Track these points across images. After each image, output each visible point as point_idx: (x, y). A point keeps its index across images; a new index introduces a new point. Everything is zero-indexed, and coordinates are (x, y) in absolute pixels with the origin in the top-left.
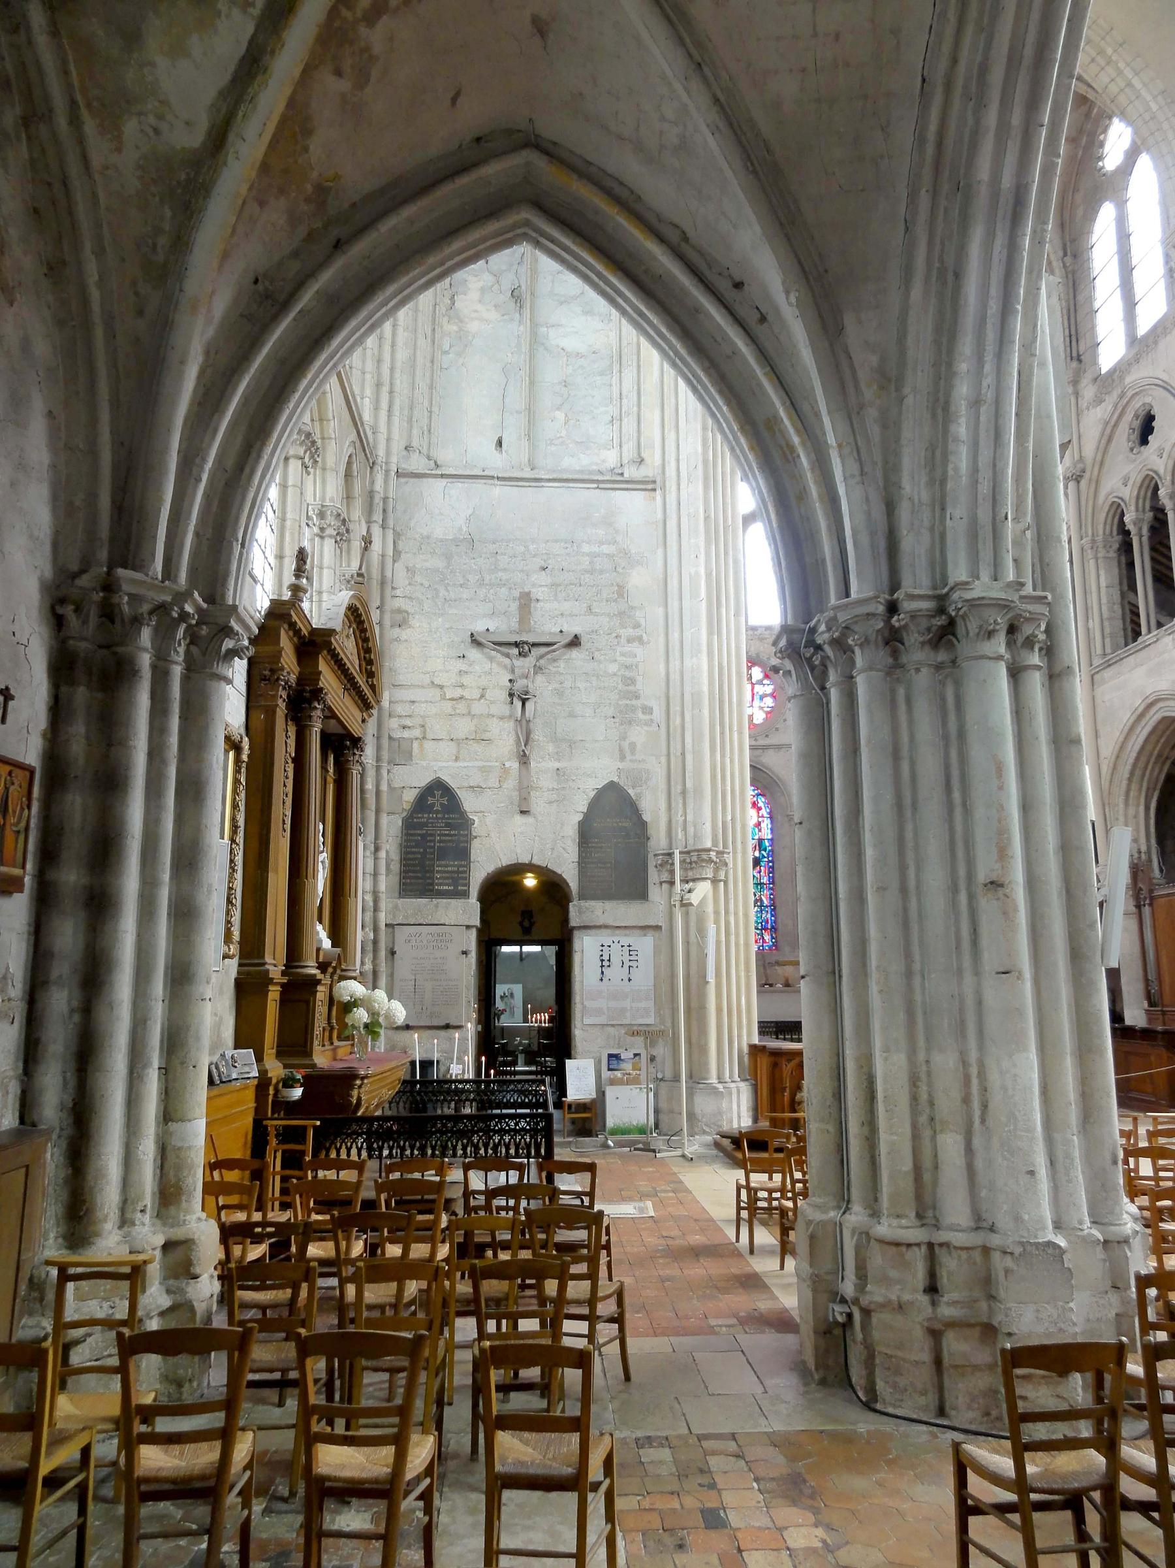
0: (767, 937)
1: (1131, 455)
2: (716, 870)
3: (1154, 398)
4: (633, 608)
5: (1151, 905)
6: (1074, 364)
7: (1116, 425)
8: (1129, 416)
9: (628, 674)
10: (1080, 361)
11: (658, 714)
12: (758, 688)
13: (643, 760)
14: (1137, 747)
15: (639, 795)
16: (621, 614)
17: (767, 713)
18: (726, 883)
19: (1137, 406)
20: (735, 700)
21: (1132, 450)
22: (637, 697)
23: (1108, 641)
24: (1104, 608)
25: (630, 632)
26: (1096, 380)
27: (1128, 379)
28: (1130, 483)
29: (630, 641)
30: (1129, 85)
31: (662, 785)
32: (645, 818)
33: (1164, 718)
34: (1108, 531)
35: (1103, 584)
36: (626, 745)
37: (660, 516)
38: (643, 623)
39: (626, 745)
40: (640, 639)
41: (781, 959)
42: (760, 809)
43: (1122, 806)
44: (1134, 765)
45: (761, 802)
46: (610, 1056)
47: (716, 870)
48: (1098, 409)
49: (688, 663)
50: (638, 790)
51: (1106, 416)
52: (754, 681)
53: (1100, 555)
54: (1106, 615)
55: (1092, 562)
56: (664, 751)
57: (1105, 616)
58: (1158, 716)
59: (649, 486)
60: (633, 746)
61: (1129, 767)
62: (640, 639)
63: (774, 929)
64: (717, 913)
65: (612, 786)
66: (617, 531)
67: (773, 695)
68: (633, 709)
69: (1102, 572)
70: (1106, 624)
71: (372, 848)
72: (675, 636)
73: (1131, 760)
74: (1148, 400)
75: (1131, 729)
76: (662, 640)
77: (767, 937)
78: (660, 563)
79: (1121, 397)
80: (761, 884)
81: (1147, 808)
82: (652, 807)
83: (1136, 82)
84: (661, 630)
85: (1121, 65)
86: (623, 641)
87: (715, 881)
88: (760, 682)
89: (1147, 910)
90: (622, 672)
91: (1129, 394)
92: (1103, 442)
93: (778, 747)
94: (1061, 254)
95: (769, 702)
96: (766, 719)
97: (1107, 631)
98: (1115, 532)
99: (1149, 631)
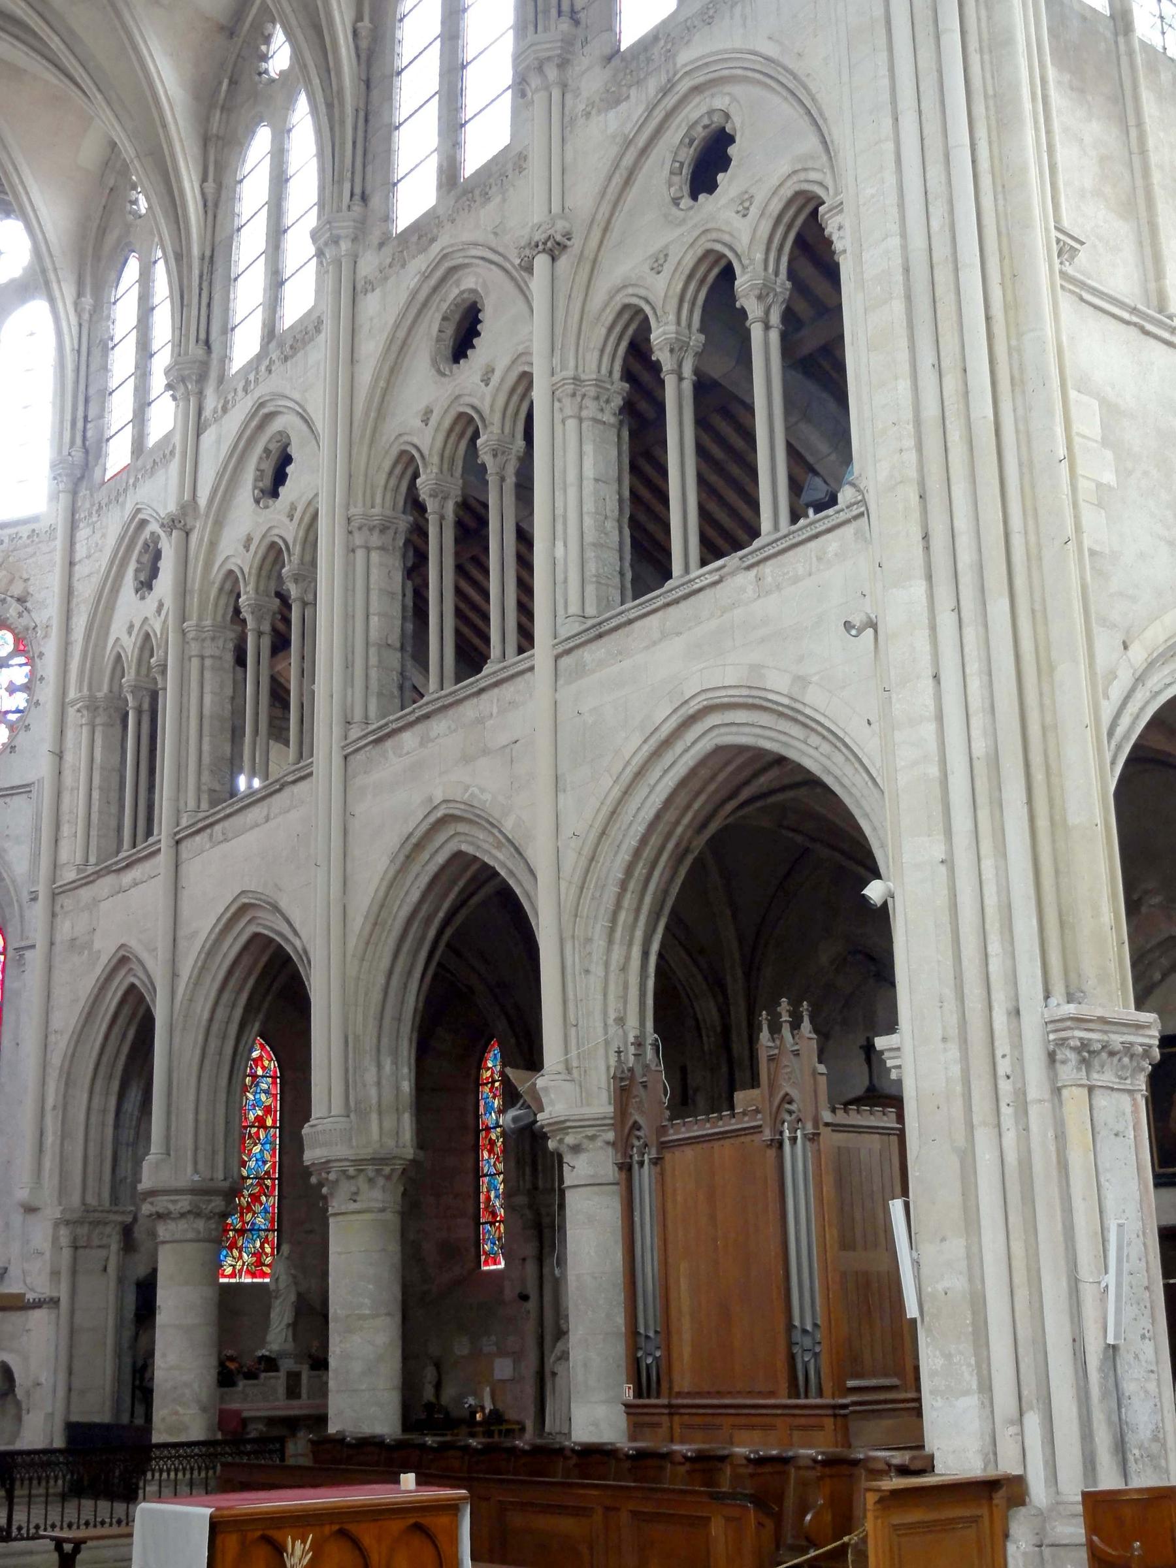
1: (674, 210)
3: (734, 99)
5: (656, 1162)
7: (644, 151)
8: (674, 135)
14: (648, 813)
19: (695, 116)
21: (676, 202)
23: (590, 589)
24: (588, 521)
26: (609, 59)
27: (685, 56)
28: (668, 268)
33: (719, 750)
34: (604, 370)
35: (589, 472)
43: (600, 943)
44: (637, 853)
48: (612, 114)
51: (629, 128)
53: (584, 413)
54: (589, 538)
55: (572, 424)
57: (589, 538)
58: (706, 745)
61: (624, 856)
69: (588, 448)
70: (590, 554)
73: (632, 841)
74: (720, 103)
75: (639, 774)
79: (666, 91)
81: (645, 954)
89: (645, 1176)
91: (684, 86)
92: (618, 180)
97: (591, 568)
98: (617, 374)
99: (687, 570)
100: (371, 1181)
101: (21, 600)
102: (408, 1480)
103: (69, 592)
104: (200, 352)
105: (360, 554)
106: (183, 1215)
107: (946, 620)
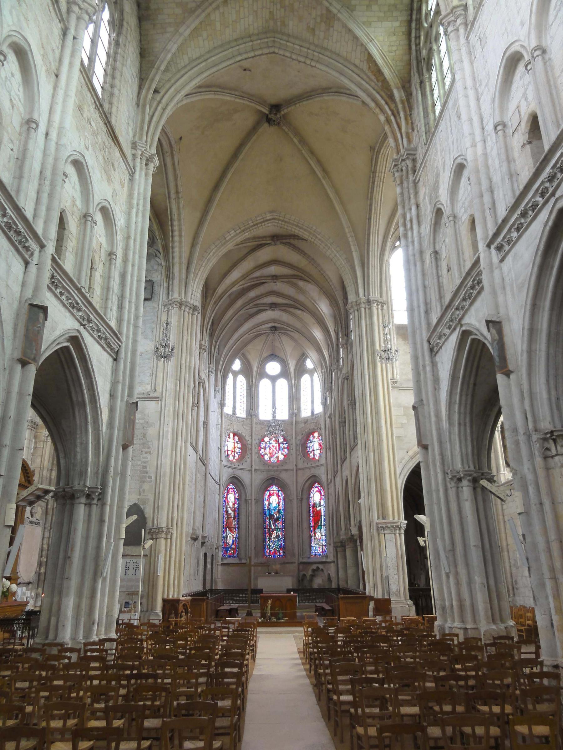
0: (281, 552)
2: (167, 534)
4: (148, 441)
6: (346, 338)
9: (145, 465)
10: (347, 336)
11: (153, 479)
12: (281, 445)
13: (147, 495)
15: (145, 508)
16: (144, 444)
17: (285, 456)
18: (171, 539)
20: (182, 473)
22: (147, 473)
25: (147, 450)
29: (146, 453)
30: (336, 256)
31: (152, 504)
32: (146, 515)
36: (141, 490)
37: (159, 410)
38: (151, 446)
39: (141, 490)
40: (150, 453)
41: (287, 561)
42: (279, 496)
45: (280, 493)
46: (126, 602)
47: (167, 534)
49: (163, 461)
50: (145, 506)
52: (280, 442)
56: (154, 492)
59: (157, 399)
60: (144, 490)
62: (150, 453)
63: (284, 549)
64: (166, 550)
65: (135, 504)
66: (145, 415)
67: (287, 448)
68: (145, 477)
71: (49, 528)
72: (160, 451)
76: (156, 452)
77: (281, 552)
78: (158, 426)
80: (279, 529)
82: (148, 512)
83: (337, 255)
84: (157, 449)
85: (333, 249)
86: (144, 453)
87: (166, 539)
88: (282, 443)
90: (143, 464)
93: (286, 470)
94: (342, 298)
95: (286, 451)
96: (284, 459)
100: (350, 542)
101: (320, 428)
102: (292, 593)
103: (325, 427)
104: (330, 385)
105: (342, 428)
106: (340, 547)
107: (364, 457)
